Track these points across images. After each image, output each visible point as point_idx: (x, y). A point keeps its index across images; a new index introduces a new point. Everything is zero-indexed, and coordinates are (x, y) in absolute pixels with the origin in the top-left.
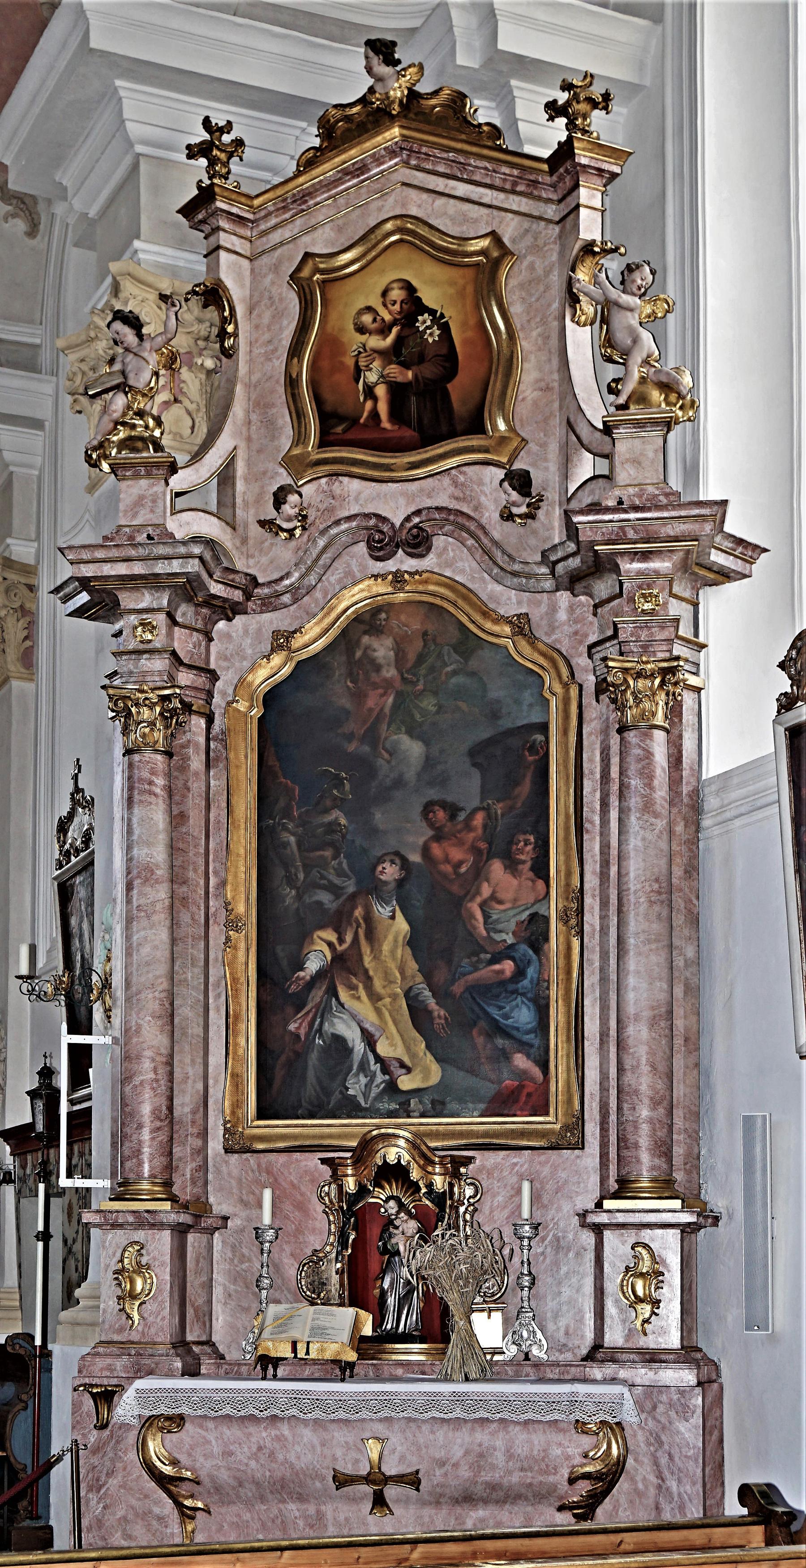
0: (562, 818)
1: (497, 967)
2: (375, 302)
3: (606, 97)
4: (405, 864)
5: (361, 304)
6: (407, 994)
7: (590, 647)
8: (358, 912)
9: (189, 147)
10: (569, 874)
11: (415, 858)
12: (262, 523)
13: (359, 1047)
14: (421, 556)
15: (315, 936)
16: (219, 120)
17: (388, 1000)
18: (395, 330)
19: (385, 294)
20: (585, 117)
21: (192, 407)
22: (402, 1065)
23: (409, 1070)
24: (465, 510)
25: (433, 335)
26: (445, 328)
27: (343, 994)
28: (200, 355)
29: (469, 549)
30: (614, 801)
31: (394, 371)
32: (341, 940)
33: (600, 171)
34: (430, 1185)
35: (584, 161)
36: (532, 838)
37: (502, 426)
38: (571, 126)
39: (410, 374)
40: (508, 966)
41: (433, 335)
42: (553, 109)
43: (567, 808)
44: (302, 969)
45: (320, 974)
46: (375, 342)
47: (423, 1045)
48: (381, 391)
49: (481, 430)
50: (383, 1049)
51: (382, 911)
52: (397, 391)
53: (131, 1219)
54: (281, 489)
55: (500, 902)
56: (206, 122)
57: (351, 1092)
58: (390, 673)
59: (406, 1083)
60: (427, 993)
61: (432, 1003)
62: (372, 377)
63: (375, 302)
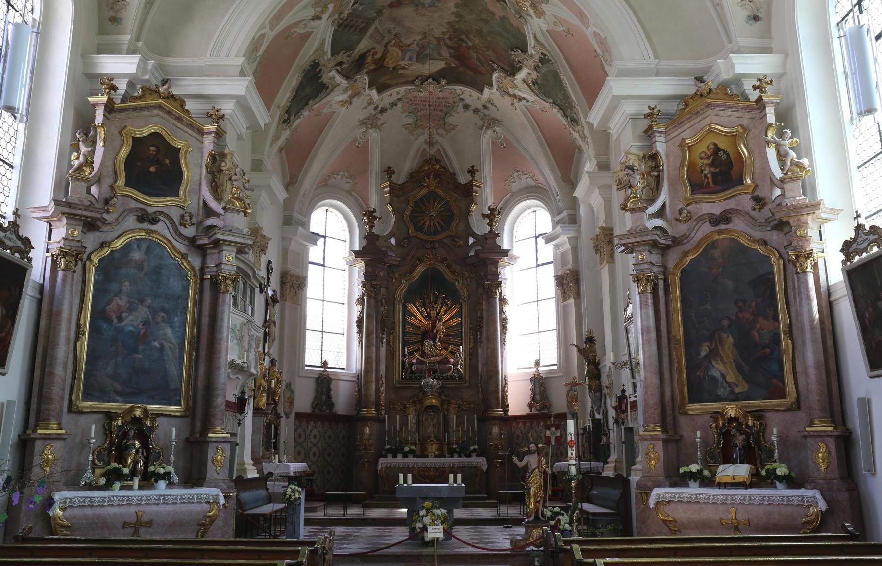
0: (781, 302)
1: (764, 351)
2: (705, 150)
3: (771, 81)
4: (730, 319)
5: (701, 151)
6: (735, 361)
7: (785, 247)
8: (717, 336)
9: (645, 115)
10: (785, 319)
11: (733, 318)
12: (676, 219)
13: (721, 379)
14: (727, 224)
15: (703, 345)
16: (652, 106)
17: (728, 364)
18: (712, 157)
19: (708, 147)
20: (765, 88)
21: (652, 187)
22: (735, 384)
23: (737, 386)
24: (739, 208)
25: (724, 157)
26: (728, 155)
27: (714, 363)
28: (653, 172)
29: (742, 220)
30: (797, 295)
31: (713, 169)
32: (711, 345)
33: (772, 103)
34: (747, 424)
35: (766, 101)
36: (772, 309)
37: (749, 181)
38: (761, 91)
39: (718, 170)
40: (768, 351)
41: (724, 157)
42: (755, 88)
43: (783, 298)
44: (700, 355)
45: (706, 357)
46: (706, 161)
47: (741, 378)
48: (709, 176)
49: (743, 184)
50: (729, 379)
51: (724, 335)
52: (714, 176)
53: (649, 437)
54: (681, 209)
55: (763, 330)
56: (649, 107)
57: (719, 394)
58: (720, 261)
59: (737, 390)
60: (741, 360)
61: (743, 364)
62: (706, 172)
63: (705, 150)
